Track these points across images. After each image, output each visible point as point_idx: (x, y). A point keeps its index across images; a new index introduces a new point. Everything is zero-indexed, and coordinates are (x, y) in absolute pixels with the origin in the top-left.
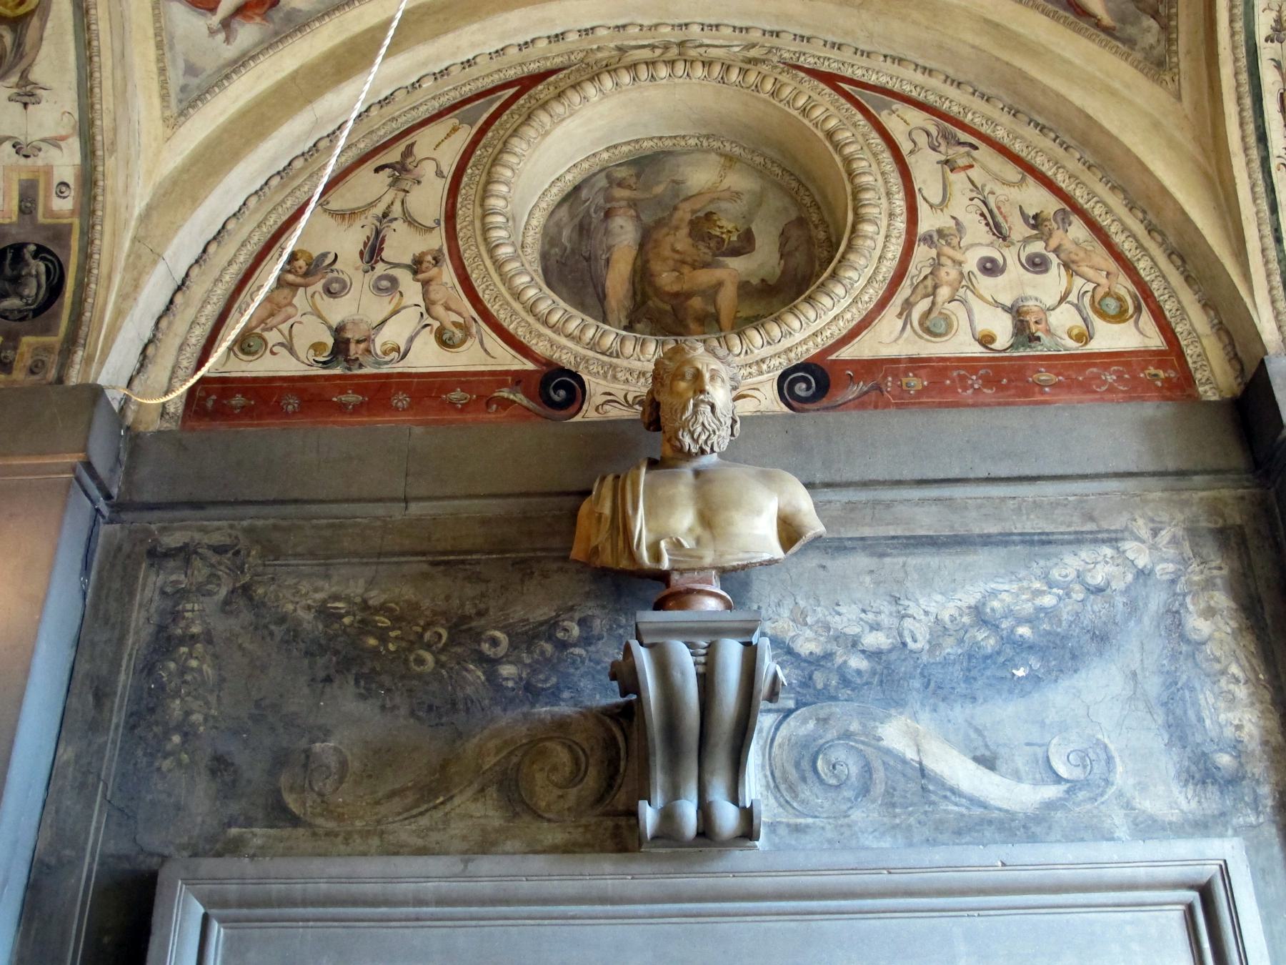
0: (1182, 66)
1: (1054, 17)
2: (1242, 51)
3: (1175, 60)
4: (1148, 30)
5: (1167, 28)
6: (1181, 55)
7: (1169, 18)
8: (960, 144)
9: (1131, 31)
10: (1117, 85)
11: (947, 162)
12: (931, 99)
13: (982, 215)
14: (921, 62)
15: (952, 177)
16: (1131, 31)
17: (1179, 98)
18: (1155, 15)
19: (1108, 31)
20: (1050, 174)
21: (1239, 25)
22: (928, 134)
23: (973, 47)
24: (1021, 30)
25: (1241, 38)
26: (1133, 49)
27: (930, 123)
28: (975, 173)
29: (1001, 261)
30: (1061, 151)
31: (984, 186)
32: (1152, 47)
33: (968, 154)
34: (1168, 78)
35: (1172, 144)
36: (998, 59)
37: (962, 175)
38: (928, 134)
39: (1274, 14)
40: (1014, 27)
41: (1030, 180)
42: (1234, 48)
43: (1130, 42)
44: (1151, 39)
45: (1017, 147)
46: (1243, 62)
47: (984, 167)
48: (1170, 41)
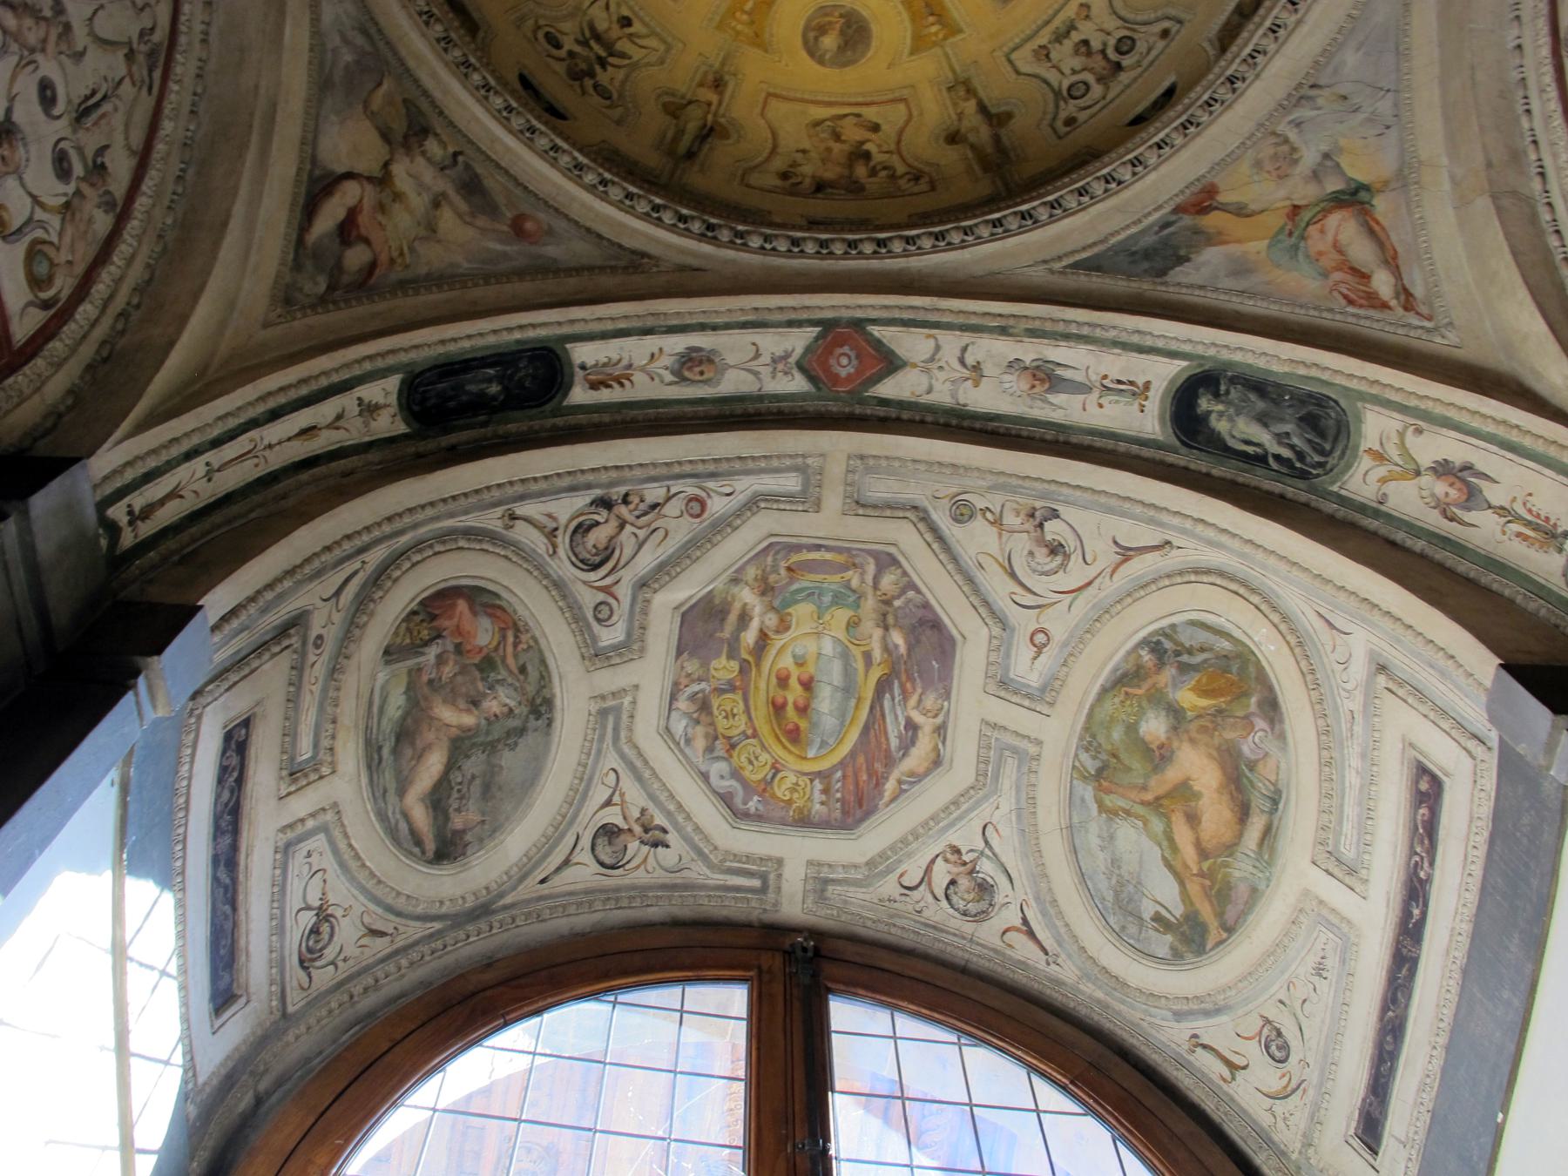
0: (296, 323)
1: (297, 182)
2: (345, 375)
3: (299, 315)
4: (316, 283)
5: (323, 302)
6: (306, 321)
7: (335, 302)
8: (150, 71)
9: (309, 265)
10: (253, 259)
11: (132, 51)
12: (183, 40)
13: (94, 93)
14: (214, 30)
15: (121, 54)
16: (309, 265)
17: (266, 325)
18: (331, 288)
19: (300, 242)
20: (144, 188)
21: (368, 366)
22: (152, 29)
23: (257, 87)
24: (275, 146)
25: (357, 371)
26: (292, 269)
27: (160, 36)
28: (127, 86)
29: (56, 112)
30: (166, 202)
31: (118, 96)
32: (301, 290)
33: (143, 81)
34: (279, 310)
35: (222, 325)
36: (252, 114)
37: (122, 70)
38: (152, 29)
39: (382, 401)
40: (276, 138)
41: (133, 162)
42: (347, 365)
43: (297, 266)
44: (308, 287)
45: (160, 147)
46: (335, 378)
47: (135, 99)
48: (313, 307)
